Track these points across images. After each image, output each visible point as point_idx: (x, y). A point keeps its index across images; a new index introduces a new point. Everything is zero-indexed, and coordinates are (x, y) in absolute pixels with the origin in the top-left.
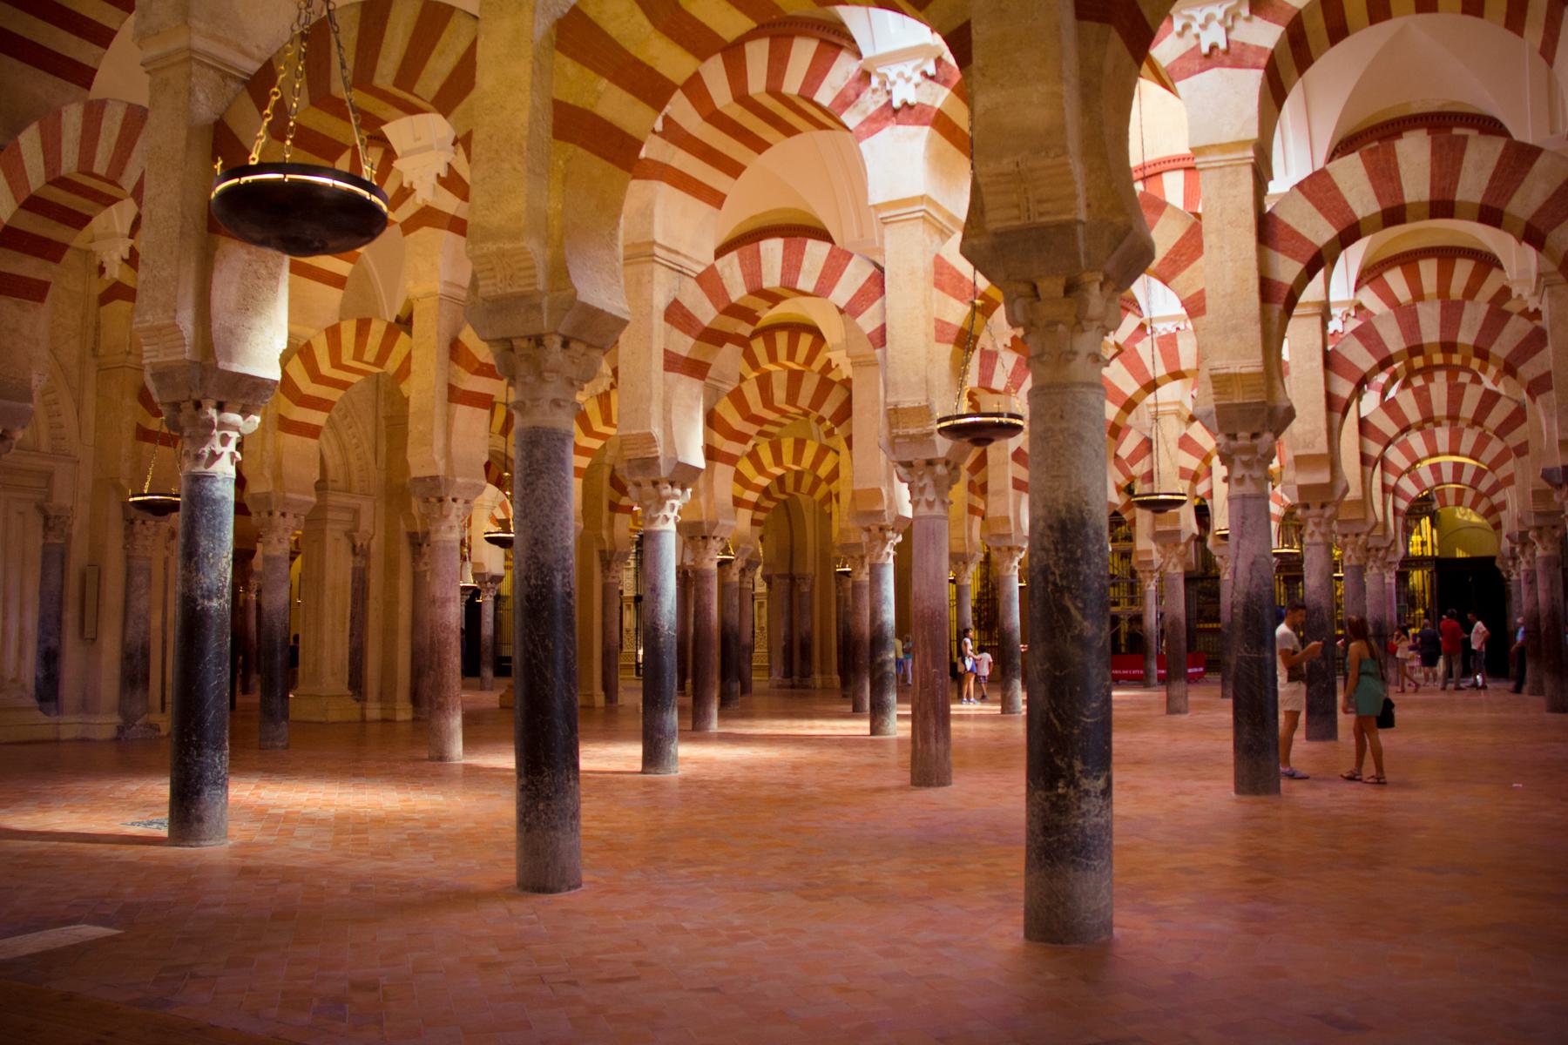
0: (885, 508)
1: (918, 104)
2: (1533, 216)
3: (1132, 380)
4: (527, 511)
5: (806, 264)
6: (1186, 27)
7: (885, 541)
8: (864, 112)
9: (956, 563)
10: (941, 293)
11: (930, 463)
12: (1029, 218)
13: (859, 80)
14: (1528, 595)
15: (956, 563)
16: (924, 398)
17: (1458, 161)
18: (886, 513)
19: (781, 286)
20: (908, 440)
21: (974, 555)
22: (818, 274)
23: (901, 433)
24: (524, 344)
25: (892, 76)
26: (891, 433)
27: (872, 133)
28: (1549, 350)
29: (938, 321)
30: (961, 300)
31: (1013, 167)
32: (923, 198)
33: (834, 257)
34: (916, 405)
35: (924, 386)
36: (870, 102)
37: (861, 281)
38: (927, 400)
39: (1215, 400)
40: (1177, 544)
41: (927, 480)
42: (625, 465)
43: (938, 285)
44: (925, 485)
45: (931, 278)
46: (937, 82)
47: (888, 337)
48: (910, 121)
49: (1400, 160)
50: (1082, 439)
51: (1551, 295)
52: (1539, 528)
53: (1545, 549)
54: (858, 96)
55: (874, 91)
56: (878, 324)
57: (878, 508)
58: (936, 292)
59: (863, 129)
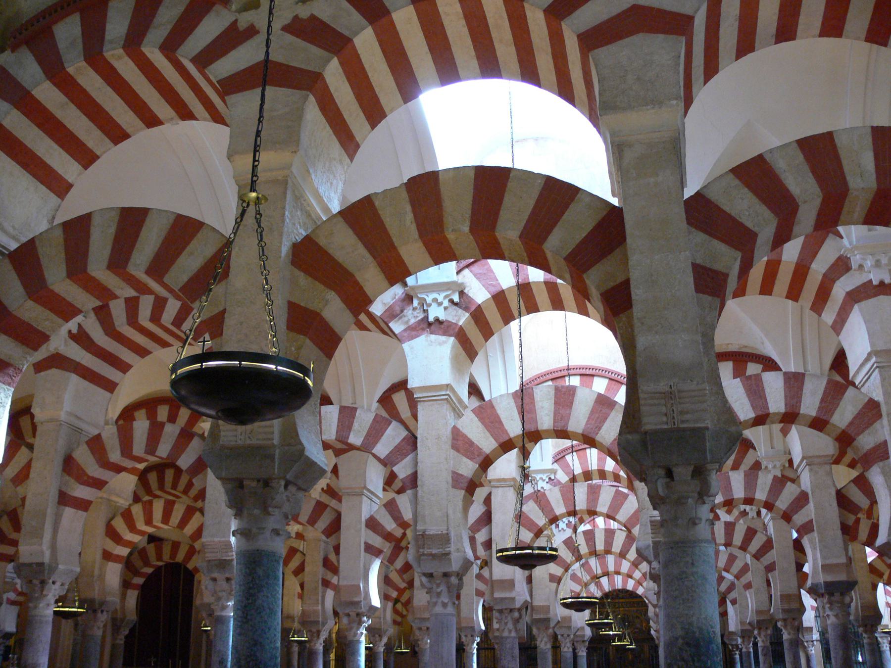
0: (362, 600)
1: (447, 321)
2: (848, 426)
4: (249, 617)
5: (356, 425)
7: (360, 623)
8: (407, 322)
9: (374, 636)
10: (456, 453)
11: (446, 575)
12: (674, 424)
13: (403, 300)
14: (764, 663)
15: (374, 636)
16: (446, 528)
17: (801, 388)
18: (362, 603)
19: (336, 439)
20: (431, 557)
21: (387, 630)
22: (365, 433)
23: (425, 552)
24: (254, 484)
25: (429, 300)
26: (418, 552)
27: (412, 338)
28: (811, 506)
29: (454, 473)
30: (471, 459)
31: (667, 389)
32: (448, 386)
33: (378, 422)
34: (440, 532)
35: (446, 519)
36: (412, 316)
37: (398, 441)
38: (448, 529)
39: (652, 538)
40: (547, 628)
41: (443, 588)
42: (205, 564)
43: (455, 447)
44: (441, 591)
45: (450, 442)
46: (460, 307)
47: (419, 483)
48: (440, 332)
49: (765, 385)
50: (706, 580)
51: (810, 470)
52: (785, 620)
53: (789, 634)
54: (402, 311)
55: (414, 309)
56: (409, 471)
57: (356, 599)
58: (453, 453)
59: (406, 334)
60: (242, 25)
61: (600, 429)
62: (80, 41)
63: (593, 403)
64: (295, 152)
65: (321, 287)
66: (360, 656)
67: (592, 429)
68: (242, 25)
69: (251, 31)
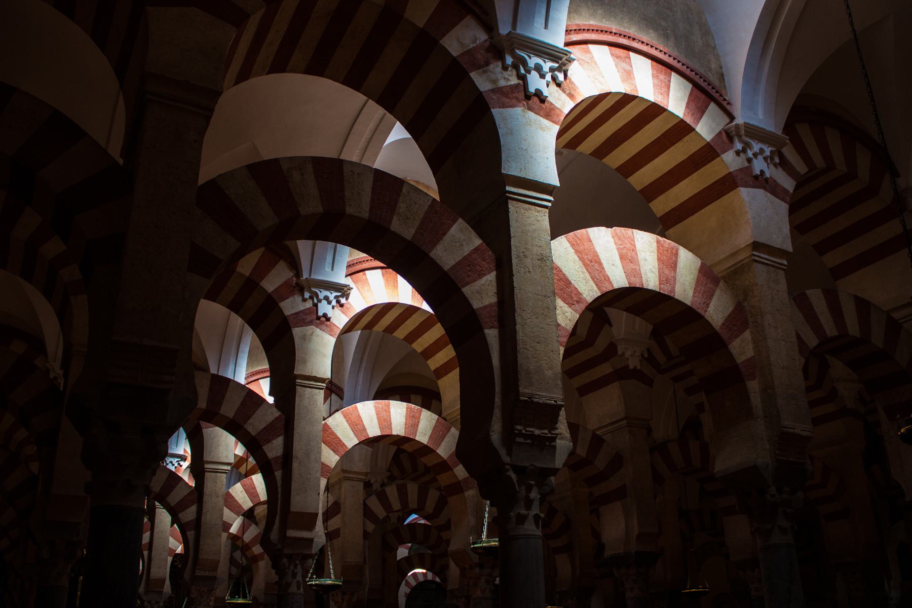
3: (352, 435)
6: (744, 151)
20: (529, 441)
23: (524, 431)
30: (570, 305)
61: (708, 306)
63: (697, 272)
67: (700, 303)
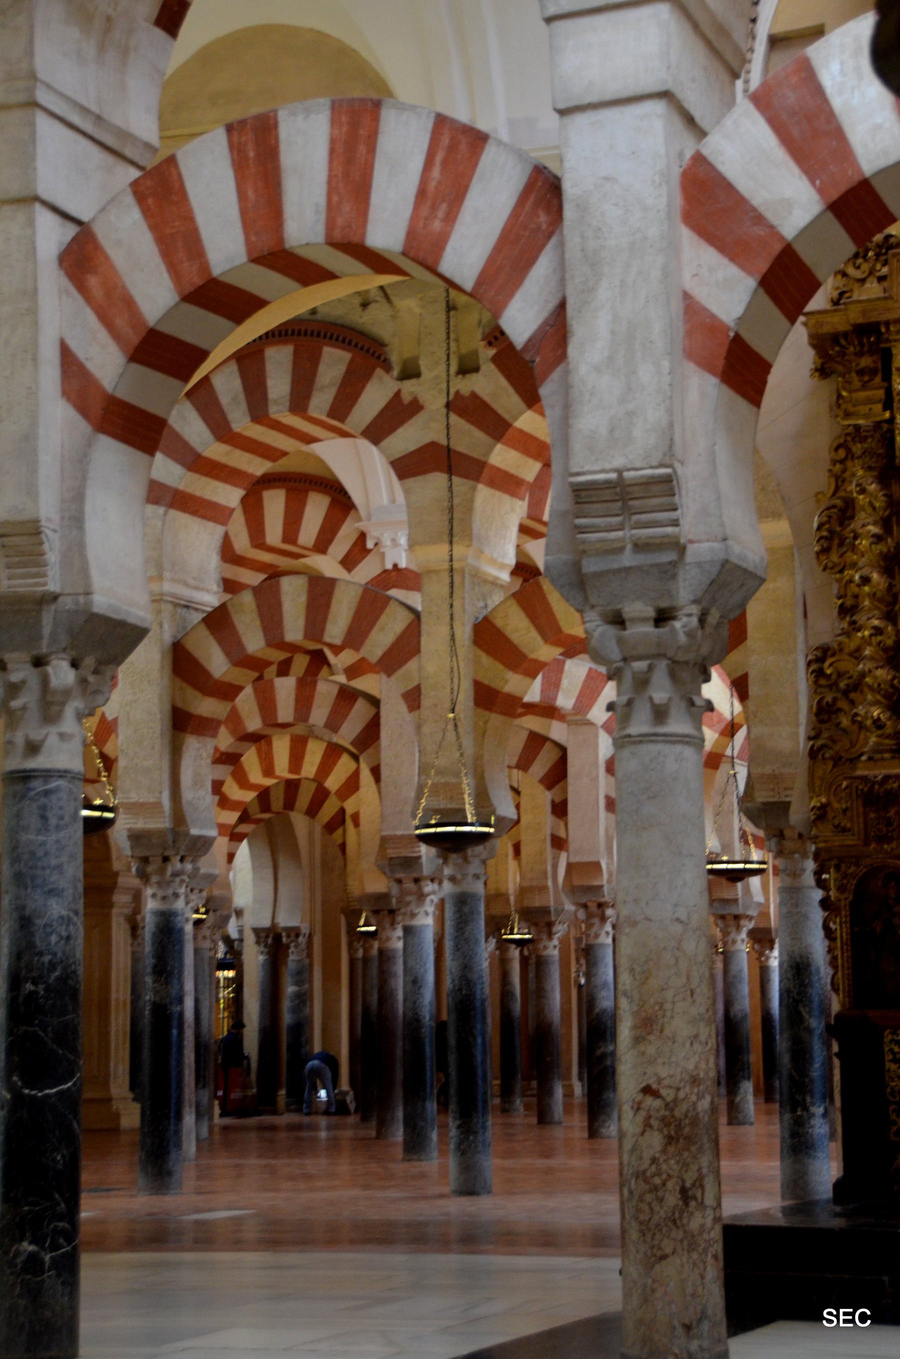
4: (459, 946)
5: (565, 683)
18: (605, 889)
22: (576, 693)
33: (592, 678)
50: (808, 918)
60: (406, 398)
62: (242, 397)
64: (469, 546)
65: (501, 667)
66: (606, 966)
68: (406, 398)
69: (415, 407)
